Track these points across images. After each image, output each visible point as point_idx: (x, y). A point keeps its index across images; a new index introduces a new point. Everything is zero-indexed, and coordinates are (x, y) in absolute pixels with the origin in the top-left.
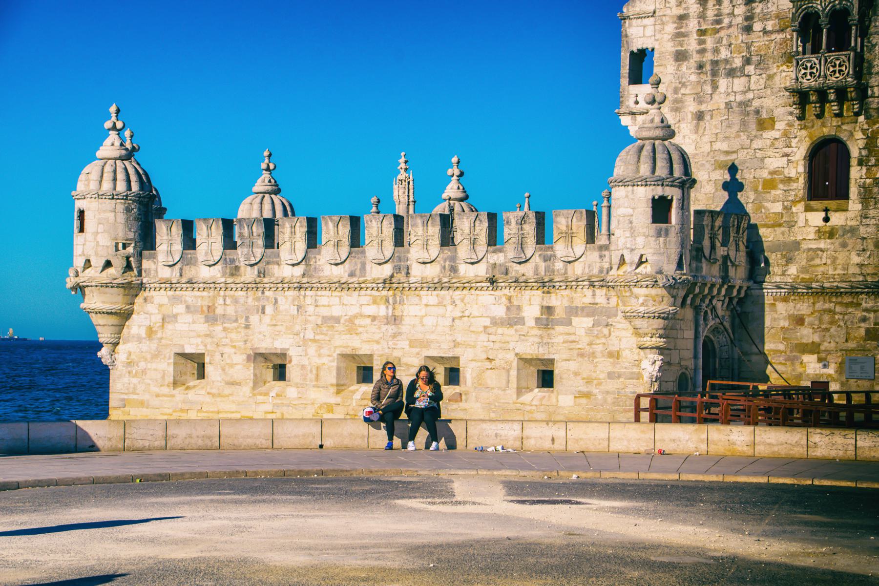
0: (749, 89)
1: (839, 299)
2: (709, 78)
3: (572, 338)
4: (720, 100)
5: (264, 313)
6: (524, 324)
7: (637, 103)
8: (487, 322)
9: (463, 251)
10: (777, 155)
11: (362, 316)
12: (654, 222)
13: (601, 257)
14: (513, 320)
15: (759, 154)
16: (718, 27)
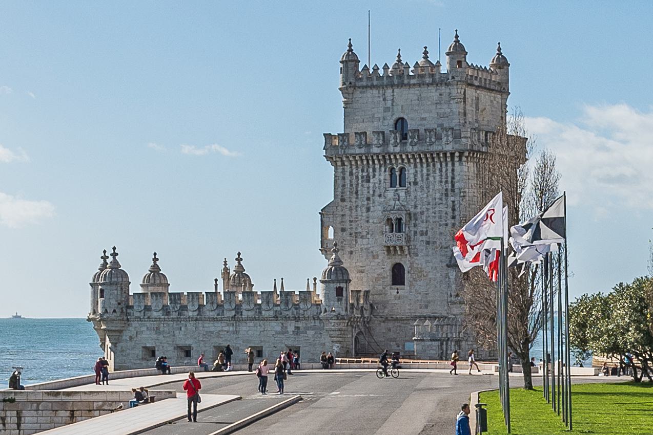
0: (369, 244)
1: (403, 322)
2: (354, 238)
3: (307, 338)
4: (358, 247)
5: (181, 329)
6: (288, 333)
7: (327, 246)
8: (274, 333)
9: (263, 307)
11: (222, 331)
12: (337, 296)
13: (317, 308)
14: (284, 332)
15: (373, 268)
16: (357, 220)
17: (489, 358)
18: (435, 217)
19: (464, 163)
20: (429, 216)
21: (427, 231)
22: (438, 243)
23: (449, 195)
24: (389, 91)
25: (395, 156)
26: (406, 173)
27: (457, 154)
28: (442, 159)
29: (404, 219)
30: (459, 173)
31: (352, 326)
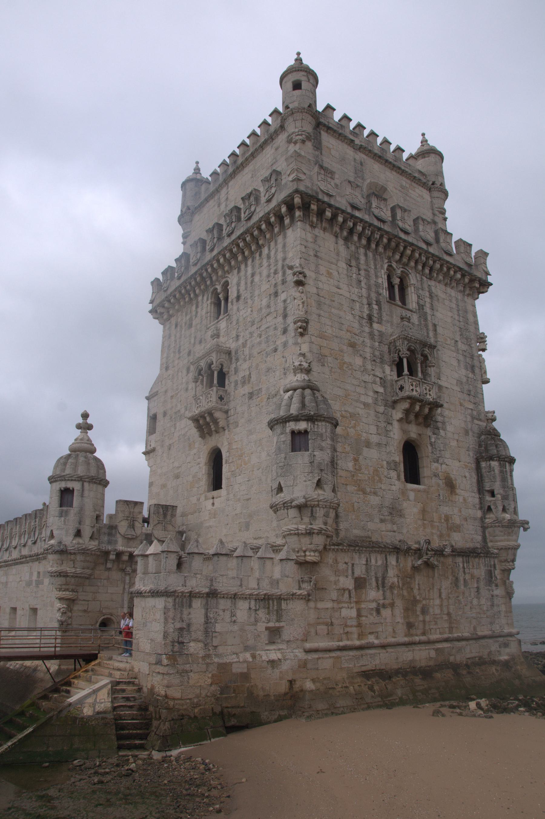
7: (150, 445)
10: (195, 464)
12: (61, 505)
17: (406, 639)
18: (260, 343)
19: (299, 223)
20: (253, 346)
21: (250, 373)
22: (263, 393)
23: (280, 291)
24: (224, 191)
25: (212, 266)
26: (229, 287)
27: (284, 209)
28: (268, 236)
29: (214, 363)
30: (292, 245)
31: (123, 570)
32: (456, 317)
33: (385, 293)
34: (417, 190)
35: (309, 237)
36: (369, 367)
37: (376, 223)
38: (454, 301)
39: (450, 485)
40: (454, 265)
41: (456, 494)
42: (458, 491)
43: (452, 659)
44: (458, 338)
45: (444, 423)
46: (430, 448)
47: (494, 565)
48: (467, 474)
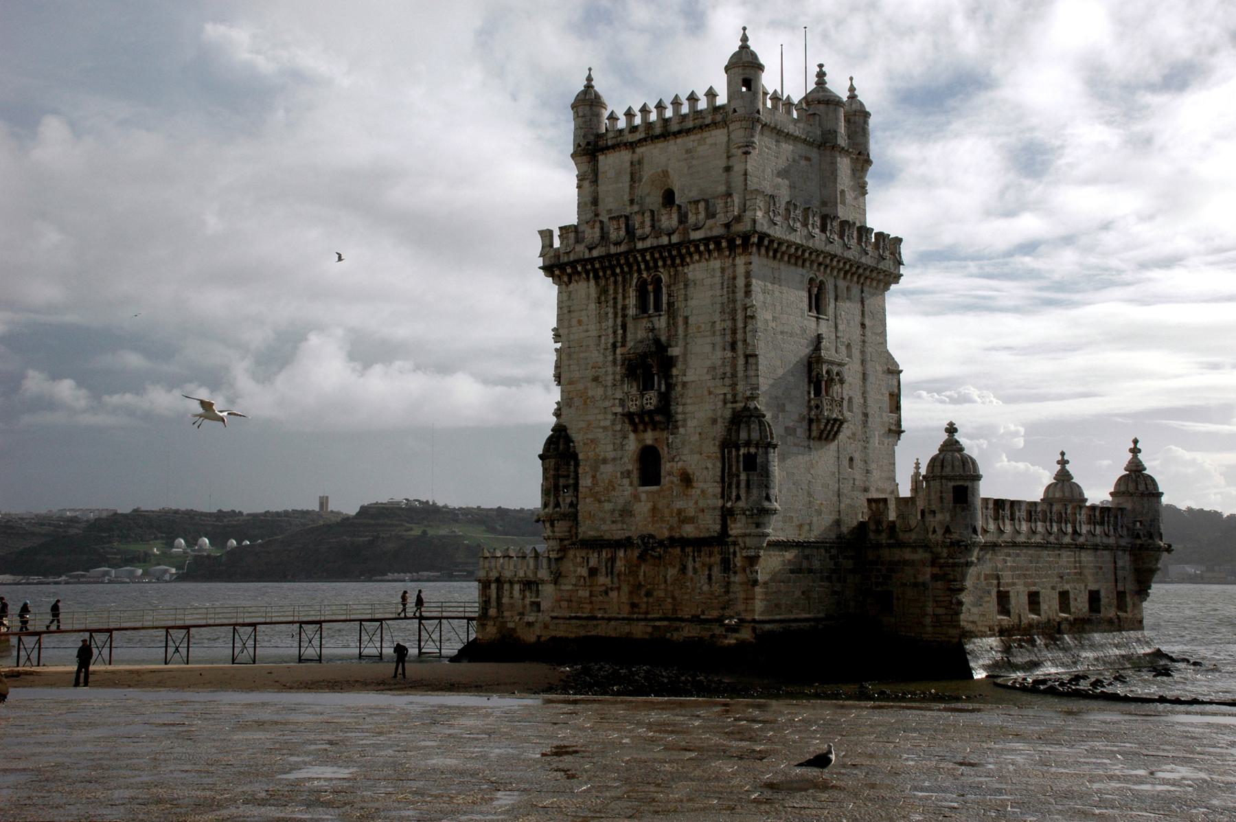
32: (718, 292)
33: (632, 311)
34: (709, 141)
35: (565, 298)
36: (610, 392)
37: (613, 250)
38: (718, 274)
39: (687, 479)
40: (700, 240)
41: (693, 488)
42: (694, 484)
43: (668, 635)
44: (717, 317)
45: (685, 420)
46: (666, 449)
47: (735, 553)
48: (710, 466)
